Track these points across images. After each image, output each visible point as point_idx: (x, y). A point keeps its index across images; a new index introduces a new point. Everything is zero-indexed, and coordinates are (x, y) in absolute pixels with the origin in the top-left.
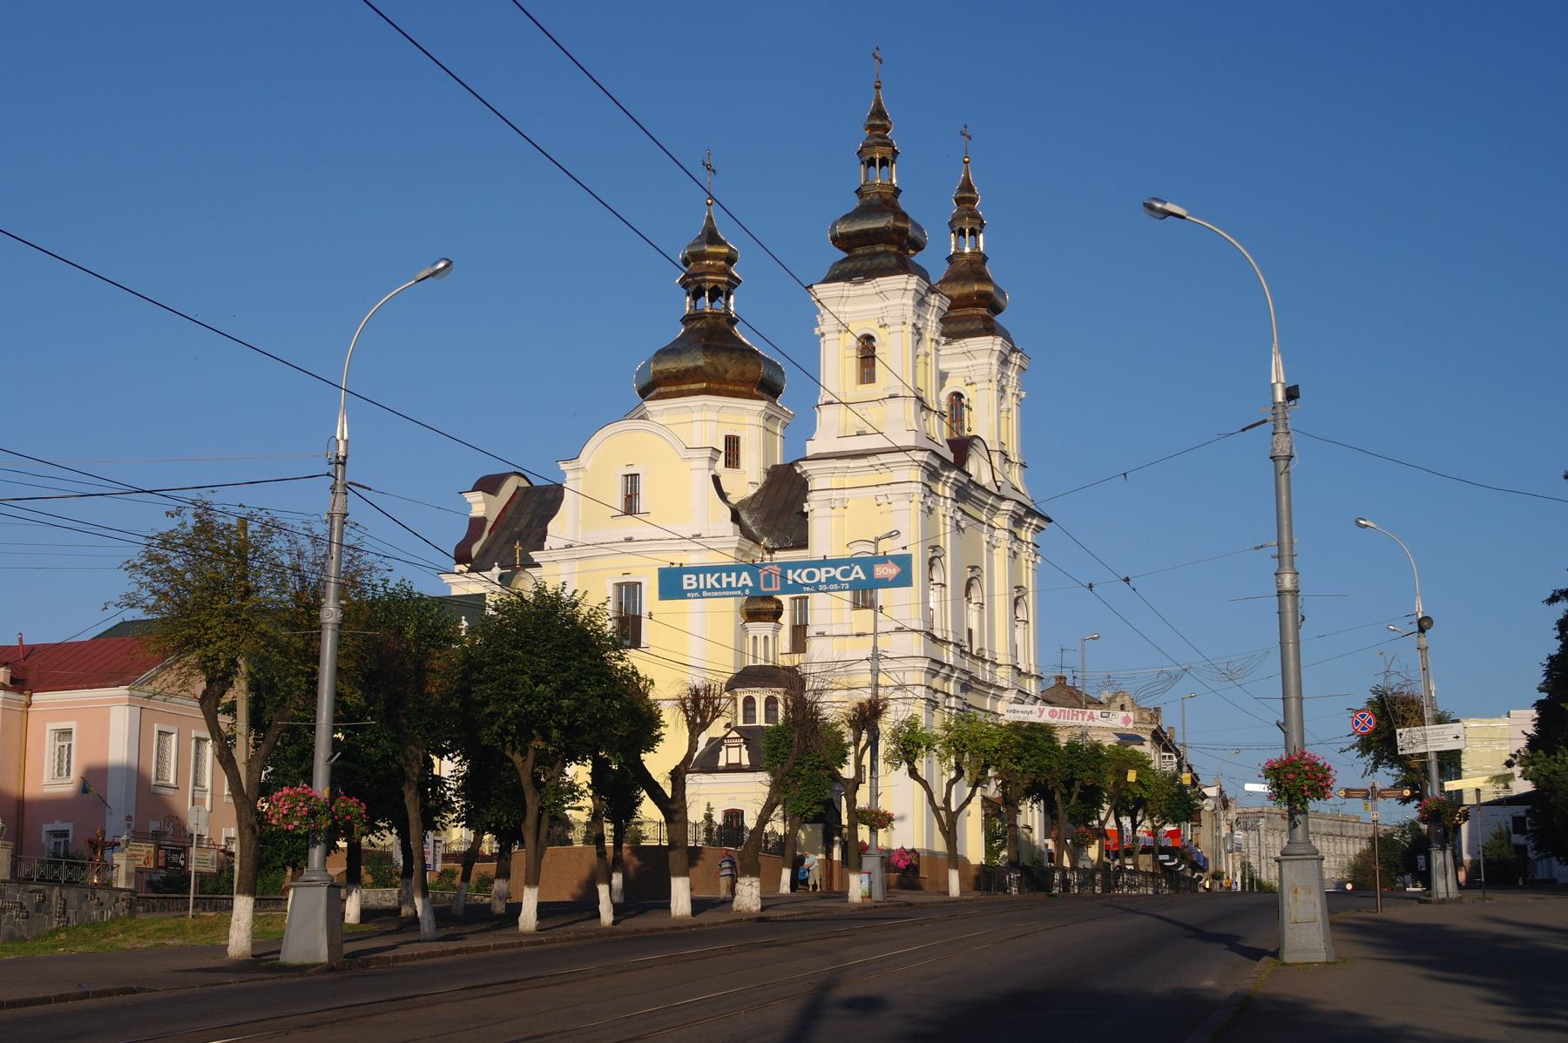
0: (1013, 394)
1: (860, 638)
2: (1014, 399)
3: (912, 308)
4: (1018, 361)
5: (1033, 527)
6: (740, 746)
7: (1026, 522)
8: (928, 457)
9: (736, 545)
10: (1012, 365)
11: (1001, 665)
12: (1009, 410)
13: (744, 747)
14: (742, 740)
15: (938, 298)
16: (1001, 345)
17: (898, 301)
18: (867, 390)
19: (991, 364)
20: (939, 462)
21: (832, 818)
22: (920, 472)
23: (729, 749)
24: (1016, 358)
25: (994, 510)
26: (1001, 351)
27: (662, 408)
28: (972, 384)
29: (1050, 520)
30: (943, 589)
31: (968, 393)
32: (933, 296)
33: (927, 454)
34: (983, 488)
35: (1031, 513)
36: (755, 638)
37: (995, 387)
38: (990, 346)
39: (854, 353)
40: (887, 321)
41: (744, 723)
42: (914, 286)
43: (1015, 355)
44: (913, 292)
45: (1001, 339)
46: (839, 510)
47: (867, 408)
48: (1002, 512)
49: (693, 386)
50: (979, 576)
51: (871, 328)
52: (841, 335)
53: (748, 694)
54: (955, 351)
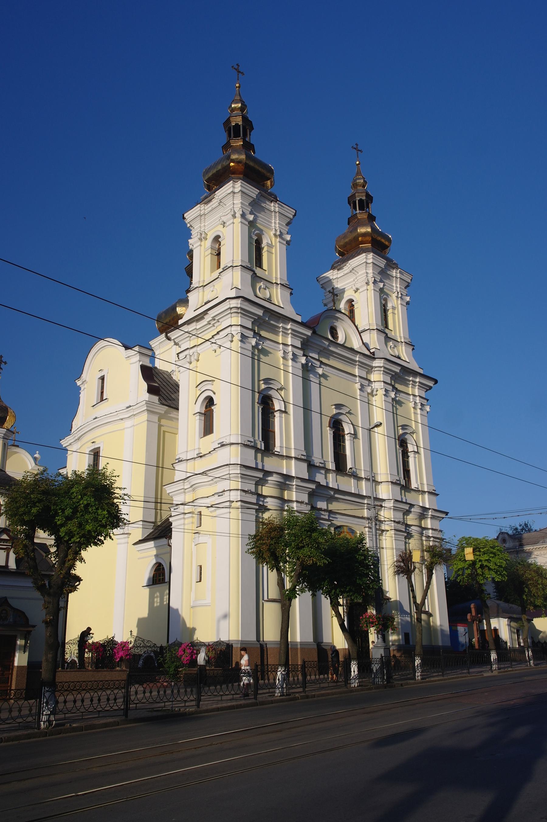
0: (397, 297)
1: (203, 458)
2: (399, 302)
3: (240, 205)
4: (398, 275)
5: (417, 384)
7: (410, 381)
8: (241, 304)
9: (145, 408)
10: (394, 279)
11: (381, 482)
12: (394, 308)
15: (277, 205)
16: (373, 258)
18: (216, 274)
19: (367, 273)
20: (262, 312)
22: (240, 318)
24: (396, 273)
25: (370, 369)
26: (373, 263)
27: (158, 343)
28: (357, 289)
29: (436, 382)
30: (283, 415)
31: (356, 297)
32: (272, 204)
33: (239, 301)
34: (352, 350)
35: (407, 371)
37: (372, 288)
38: (365, 260)
42: (240, 189)
43: (394, 271)
44: (240, 194)
45: (372, 254)
47: (214, 286)
48: (376, 369)
50: (349, 413)
51: (219, 230)
54: (346, 272)
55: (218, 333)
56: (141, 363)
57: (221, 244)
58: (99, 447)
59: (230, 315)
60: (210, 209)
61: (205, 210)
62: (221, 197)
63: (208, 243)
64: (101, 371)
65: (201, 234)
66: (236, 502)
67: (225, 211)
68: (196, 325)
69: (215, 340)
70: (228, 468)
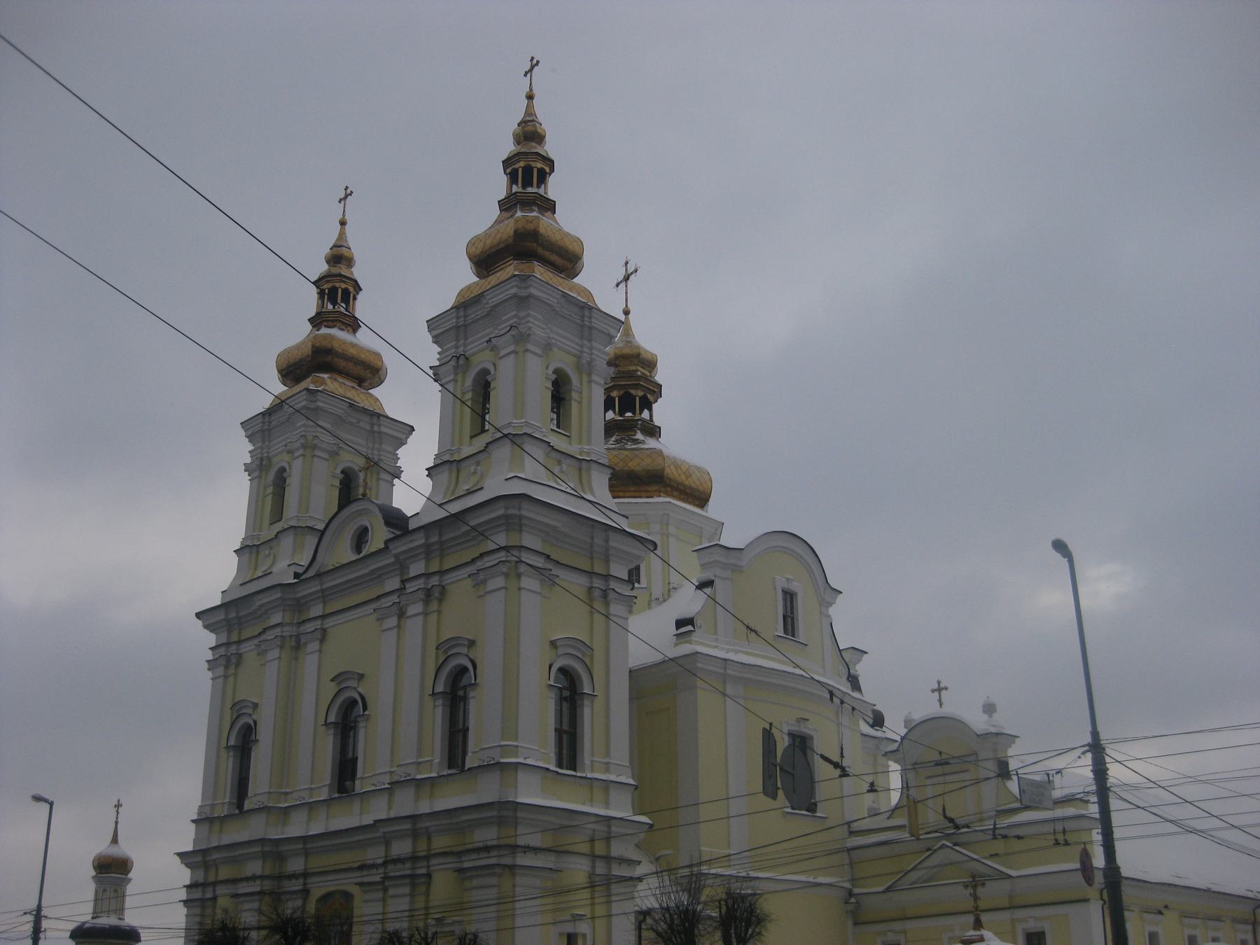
39: (270, 490)
46: (232, 670)
55: (265, 630)
61: (270, 422)
63: (271, 476)
65: (262, 459)
67: (293, 434)
69: (259, 642)
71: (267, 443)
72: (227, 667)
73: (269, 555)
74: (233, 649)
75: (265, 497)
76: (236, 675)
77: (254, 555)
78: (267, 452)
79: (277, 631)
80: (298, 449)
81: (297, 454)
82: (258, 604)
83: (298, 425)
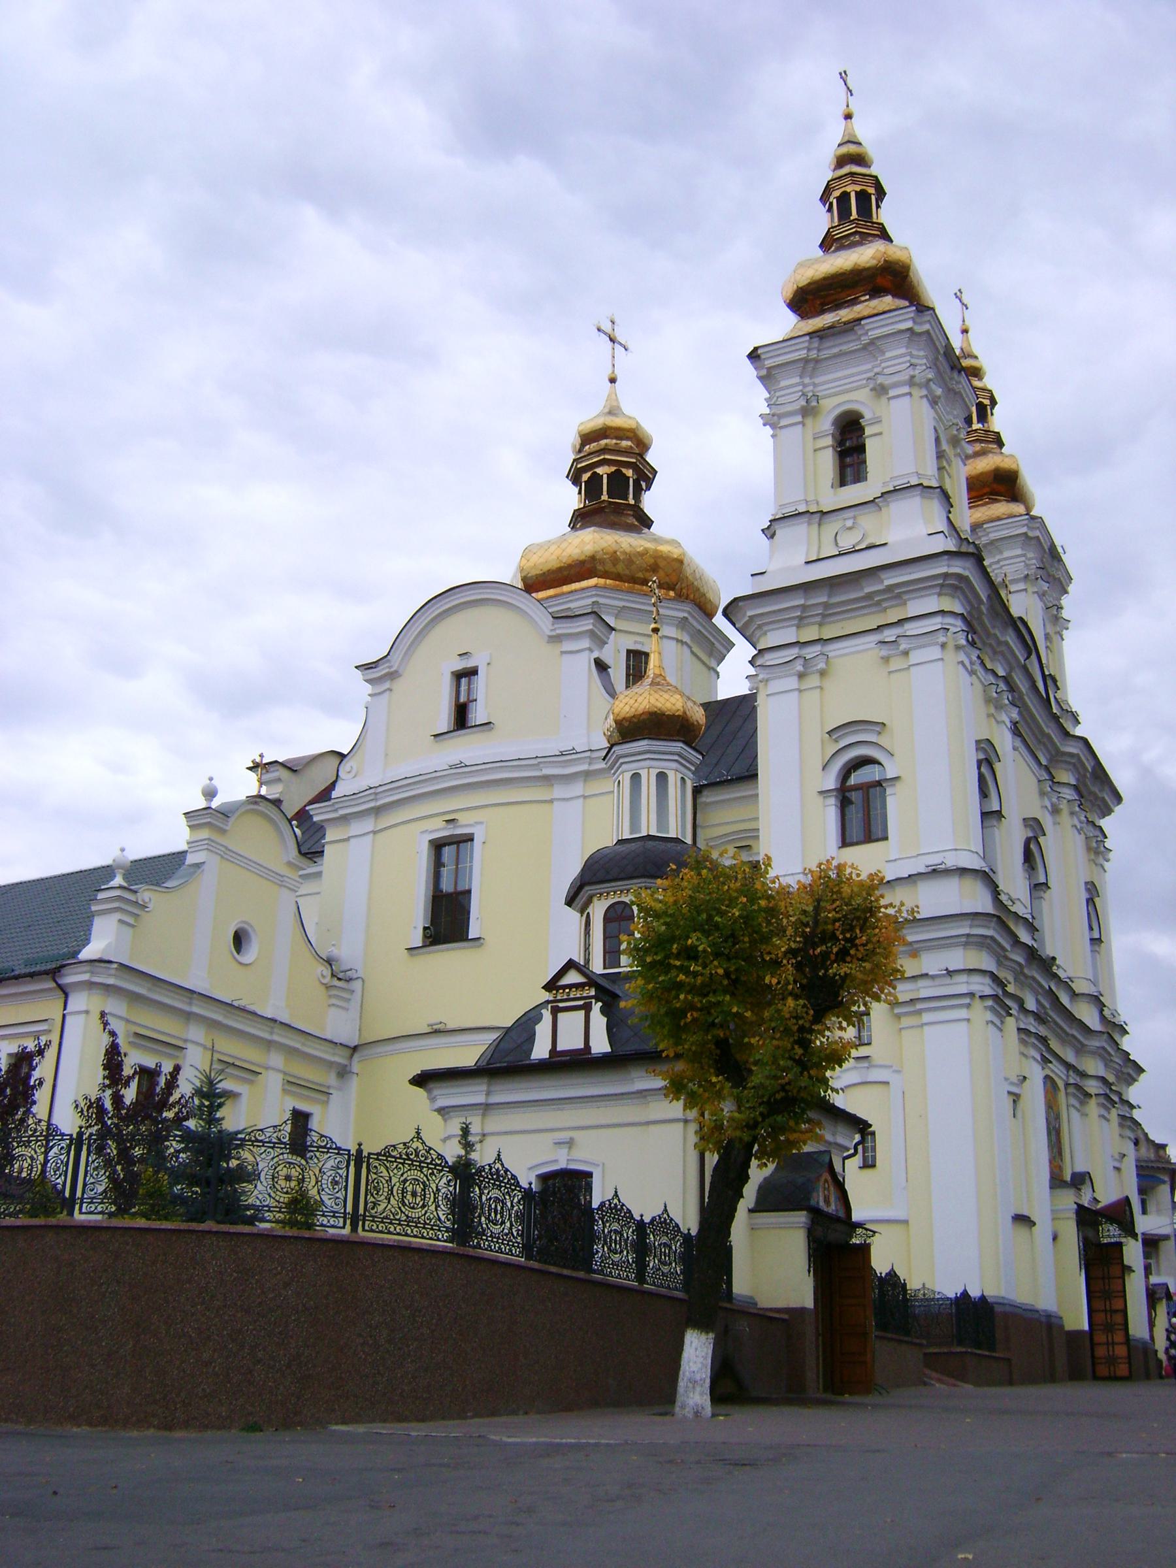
6: (587, 1008)
13: (597, 1007)
14: (593, 993)
17: (903, 351)
21: (827, 1202)
23: (560, 1015)
36: (636, 777)
39: (829, 441)
40: (880, 380)
41: (605, 968)
46: (813, 681)
47: (854, 518)
49: (585, 584)
51: (860, 400)
52: (809, 421)
53: (616, 900)
55: (900, 622)
56: (596, 654)
57: (868, 431)
58: (473, 834)
59: (937, 590)
60: (835, 350)
61: (819, 350)
62: (874, 334)
63: (826, 424)
64: (465, 657)
66: (980, 997)
68: (830, 596)
70: (969, 922)
71: (807, 380)
72: (801, 676)
73: (850, 528)
74: (810, 652)
75: (815, 451)
76: (821, 688)
77: (815, 526)
78: (813, 391)
79: (935, 623)
80: (896, 385)
81: (892, 393)
82: (887, 583)
83: (888, 355)
